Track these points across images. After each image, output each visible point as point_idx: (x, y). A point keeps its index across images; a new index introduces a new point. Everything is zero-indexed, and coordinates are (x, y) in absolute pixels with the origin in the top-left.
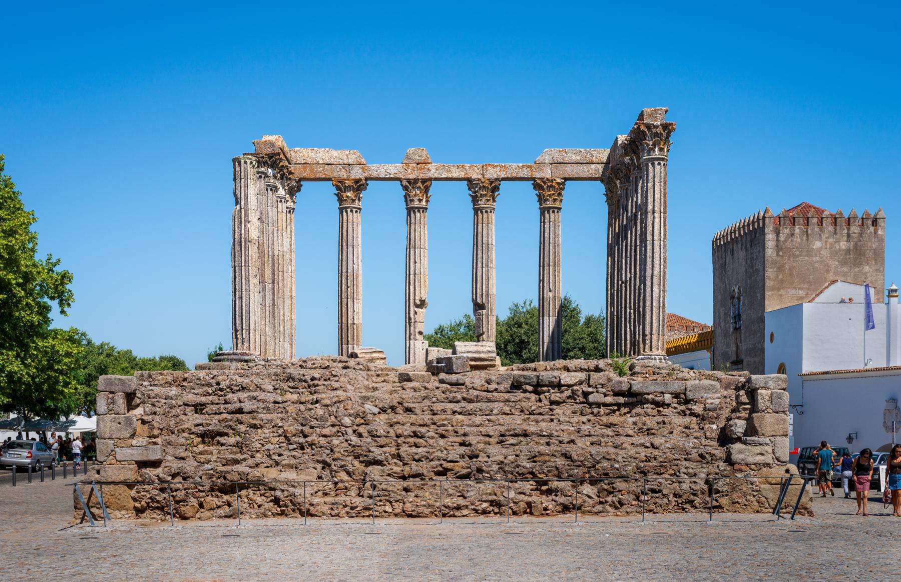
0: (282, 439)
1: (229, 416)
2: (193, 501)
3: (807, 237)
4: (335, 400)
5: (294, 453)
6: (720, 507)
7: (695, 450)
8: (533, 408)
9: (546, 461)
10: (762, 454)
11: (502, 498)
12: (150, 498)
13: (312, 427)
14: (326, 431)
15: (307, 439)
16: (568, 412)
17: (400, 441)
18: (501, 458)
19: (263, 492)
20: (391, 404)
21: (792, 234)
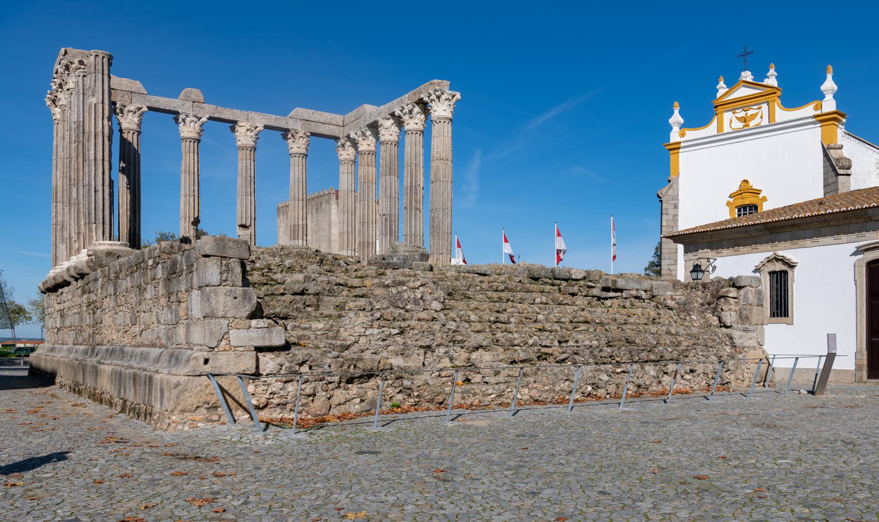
0: (382, 323)
1: (298, 297)
8: (561, 299)
14: (423, 315)
15: (408, 323)
17: (494, 326)
19: (390, 382)
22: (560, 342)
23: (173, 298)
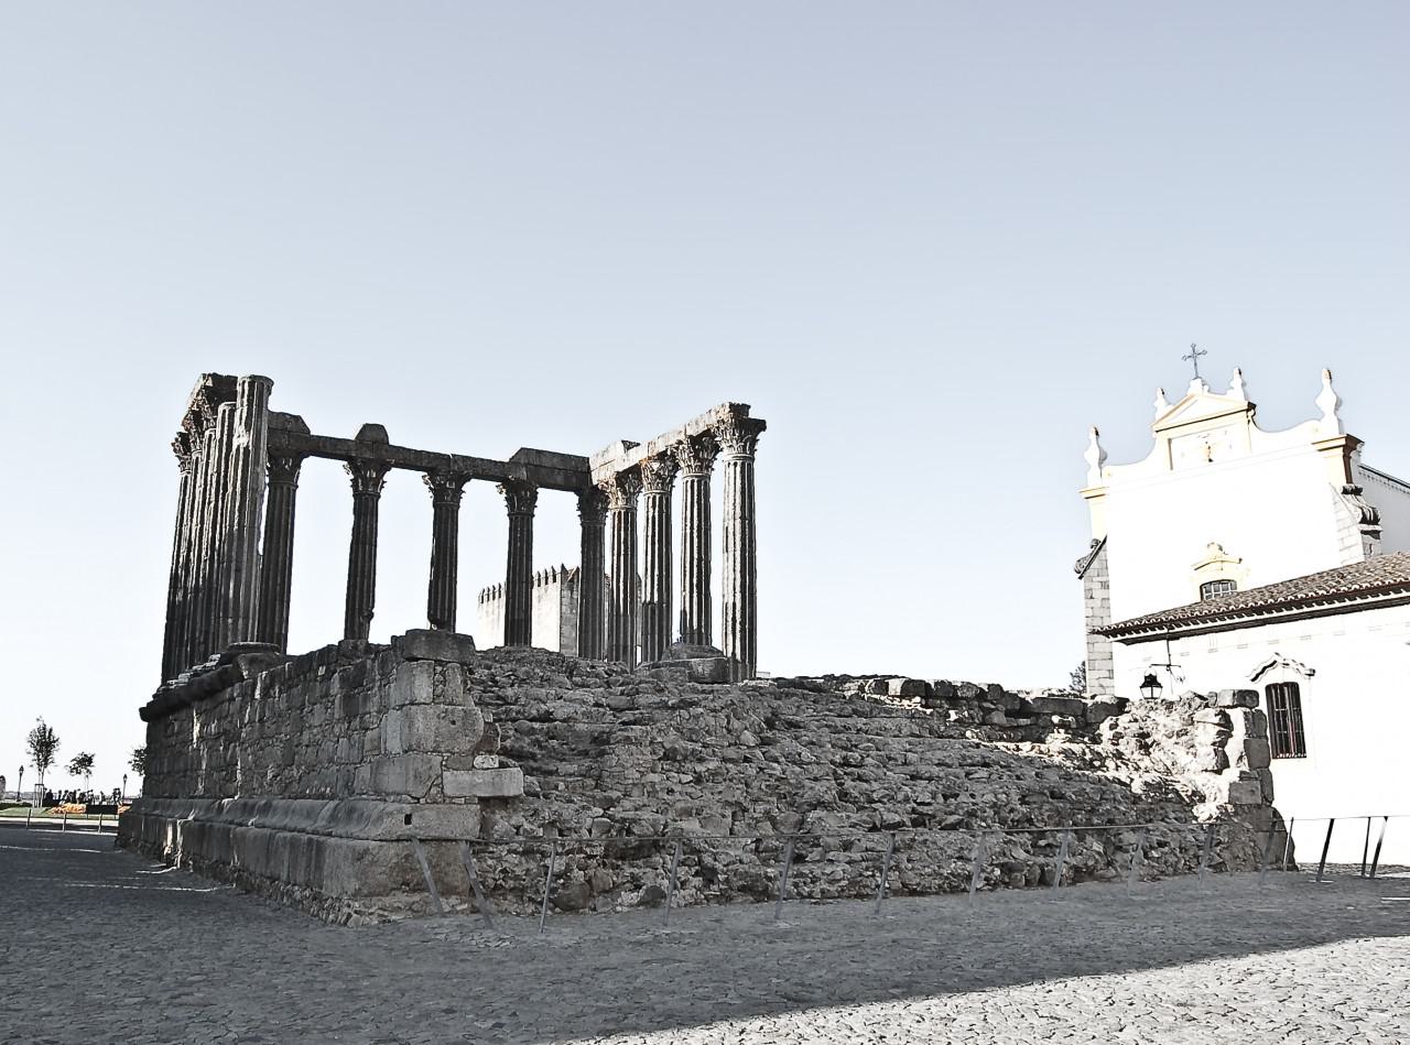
1: (537, 725)
12: (504, 871)
13: (705, 746)
14: (731, 753)
22: (946, 797)
23: (356, 723)
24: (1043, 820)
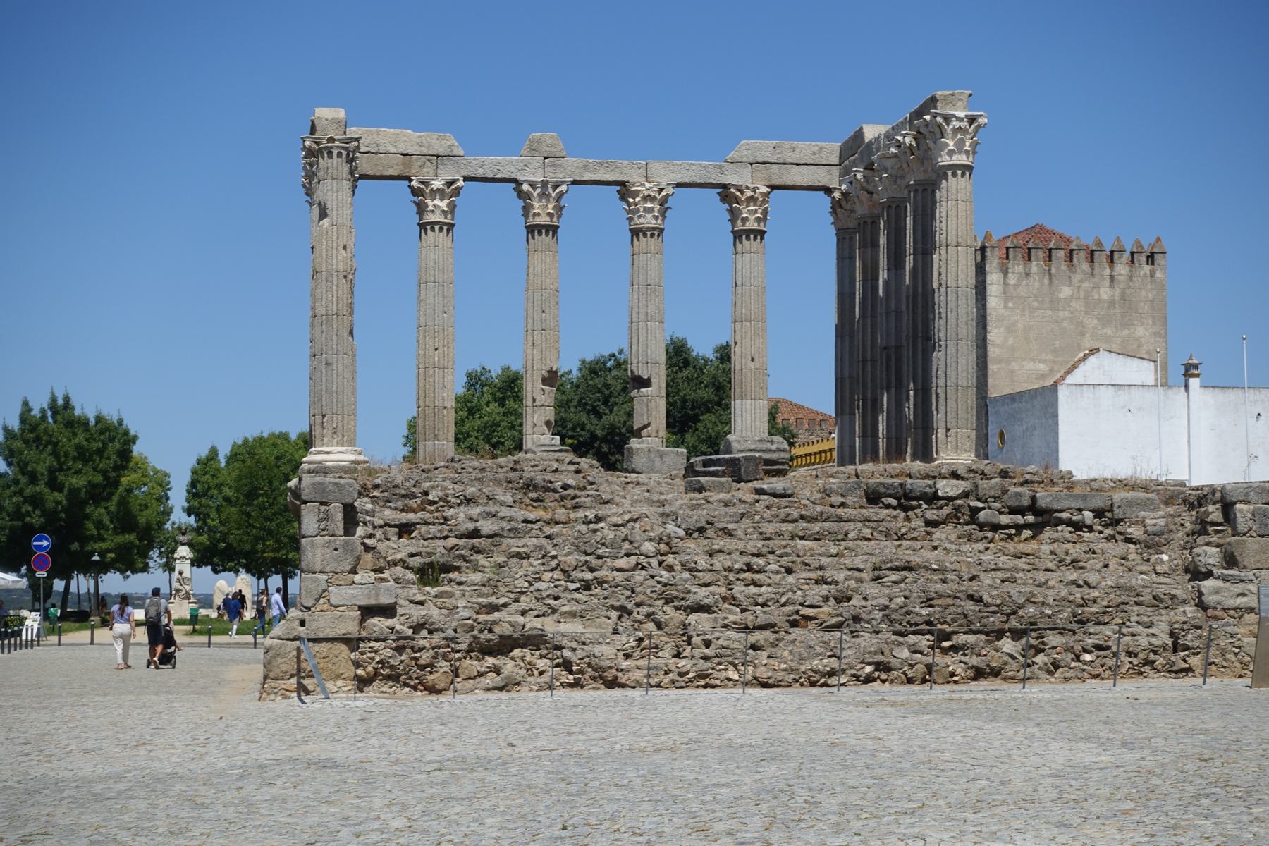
0: (557, 574)
2: (444, 666)
3: (1050, 279)
4: (627, 517)
5: (577, 595)
6: (1188, 671)
7: (1148, 590)
8: (903, 530)
9: (946, 607)
10: (1244, 595)
11: (893, 660)
12: (380, 662)
13: (599, 557)
14: (622, 563)
15: (595, 574)
16: (953, 537)
17: (732, 577)
18: (887, 603)
20: (699, 525)
21: (1028, 275)
24: (945, 622)
